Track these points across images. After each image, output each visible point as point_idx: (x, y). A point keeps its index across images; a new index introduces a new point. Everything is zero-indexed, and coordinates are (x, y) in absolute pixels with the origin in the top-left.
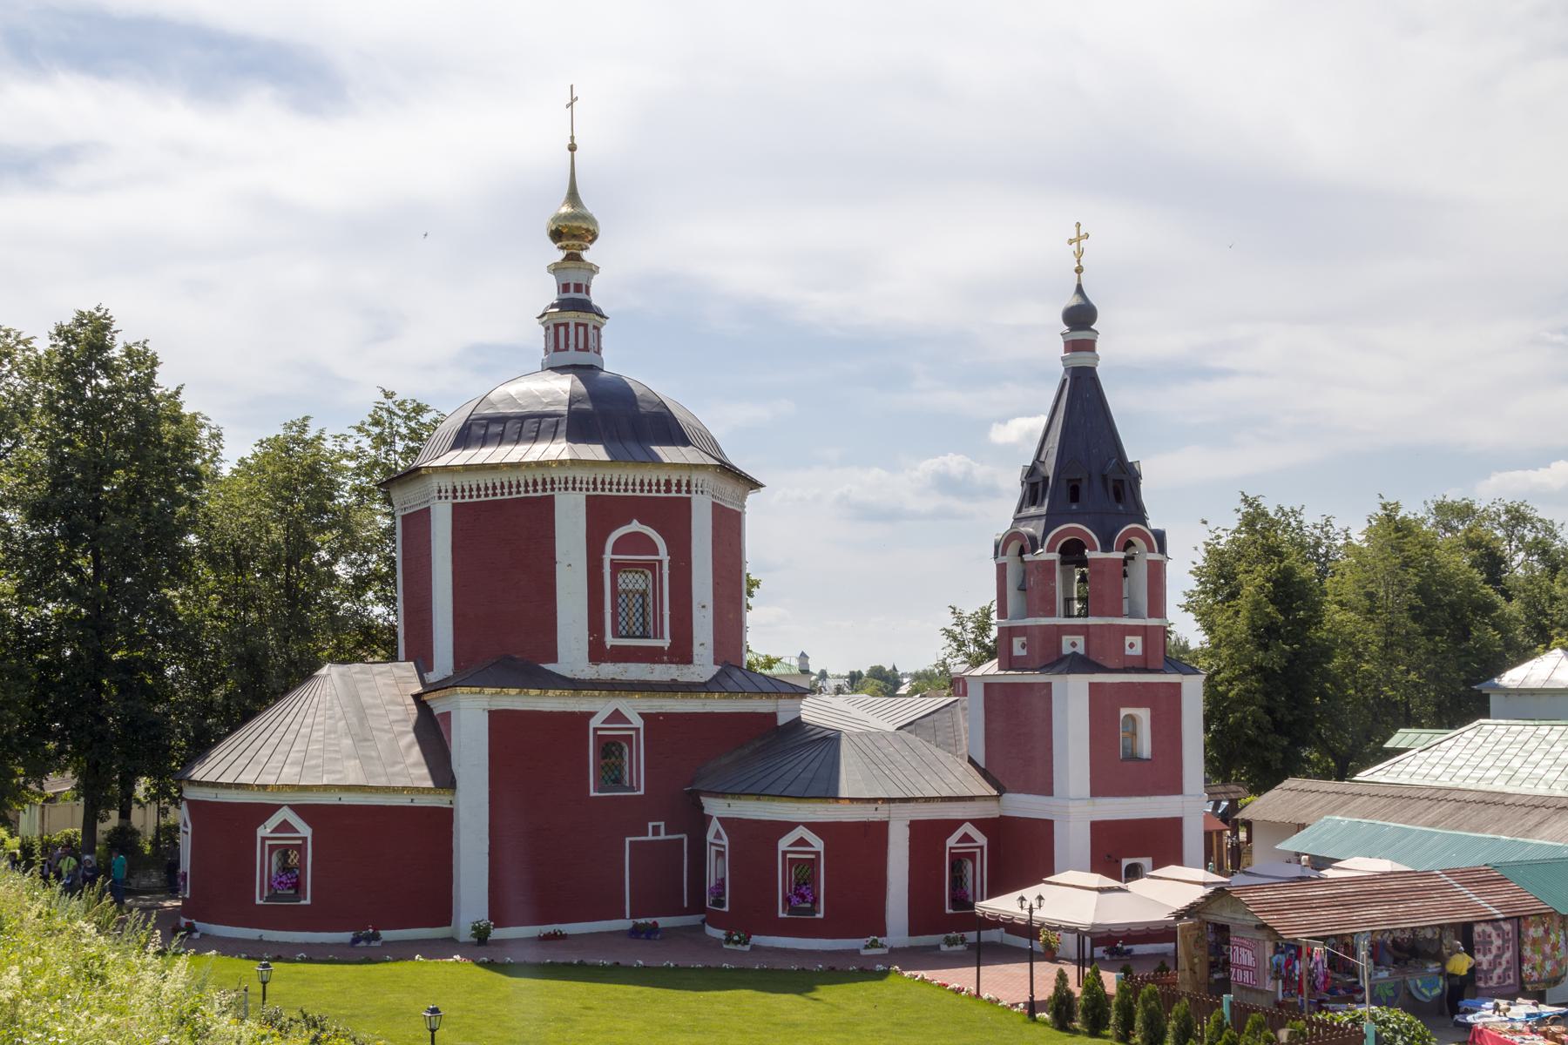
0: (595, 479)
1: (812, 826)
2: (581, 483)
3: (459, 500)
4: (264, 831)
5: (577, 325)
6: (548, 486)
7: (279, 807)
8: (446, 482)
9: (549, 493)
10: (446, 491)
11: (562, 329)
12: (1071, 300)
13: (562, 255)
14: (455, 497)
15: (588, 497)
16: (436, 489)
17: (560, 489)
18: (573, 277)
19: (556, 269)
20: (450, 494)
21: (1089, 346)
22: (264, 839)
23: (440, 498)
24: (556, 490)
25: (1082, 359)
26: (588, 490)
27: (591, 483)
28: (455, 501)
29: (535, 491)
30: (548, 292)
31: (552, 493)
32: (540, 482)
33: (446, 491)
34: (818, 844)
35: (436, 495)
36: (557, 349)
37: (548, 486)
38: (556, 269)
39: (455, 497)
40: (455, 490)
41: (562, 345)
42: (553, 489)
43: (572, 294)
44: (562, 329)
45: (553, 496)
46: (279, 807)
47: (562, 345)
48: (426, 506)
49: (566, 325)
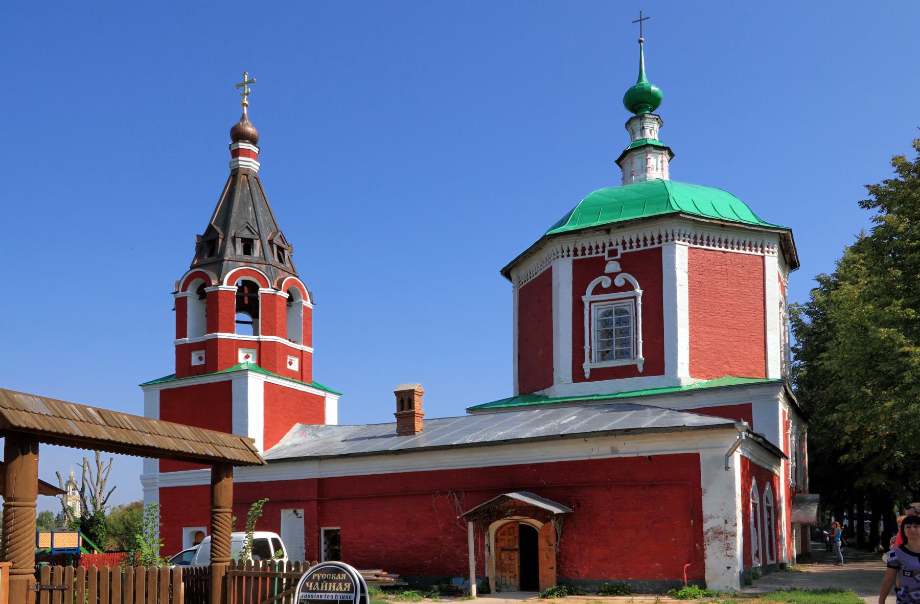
0: (695, 236)
2: (684, 236)
3: (580, 257)
6: (656, 241)
8: (569, 243)
9: (656, 245)
10: (569, 251)
14: (576, 254)
15: (690, 248)
16: (559, 250)
17: (667, 241)
20: (571, 253)
23: (563, 256)
24: (664, 242)
26: (689, 242)
27: (692, 238)
28: (576, 258)
29: (646, 245)
31: (659, 246)
32: (649, 238)
33: (569, 251)
35: (560, 254)
37: (656, 241)
39: (576, 254)
40: (576, 250)
42: (660, 242)
45: (660, 249)
48: (549, 266)
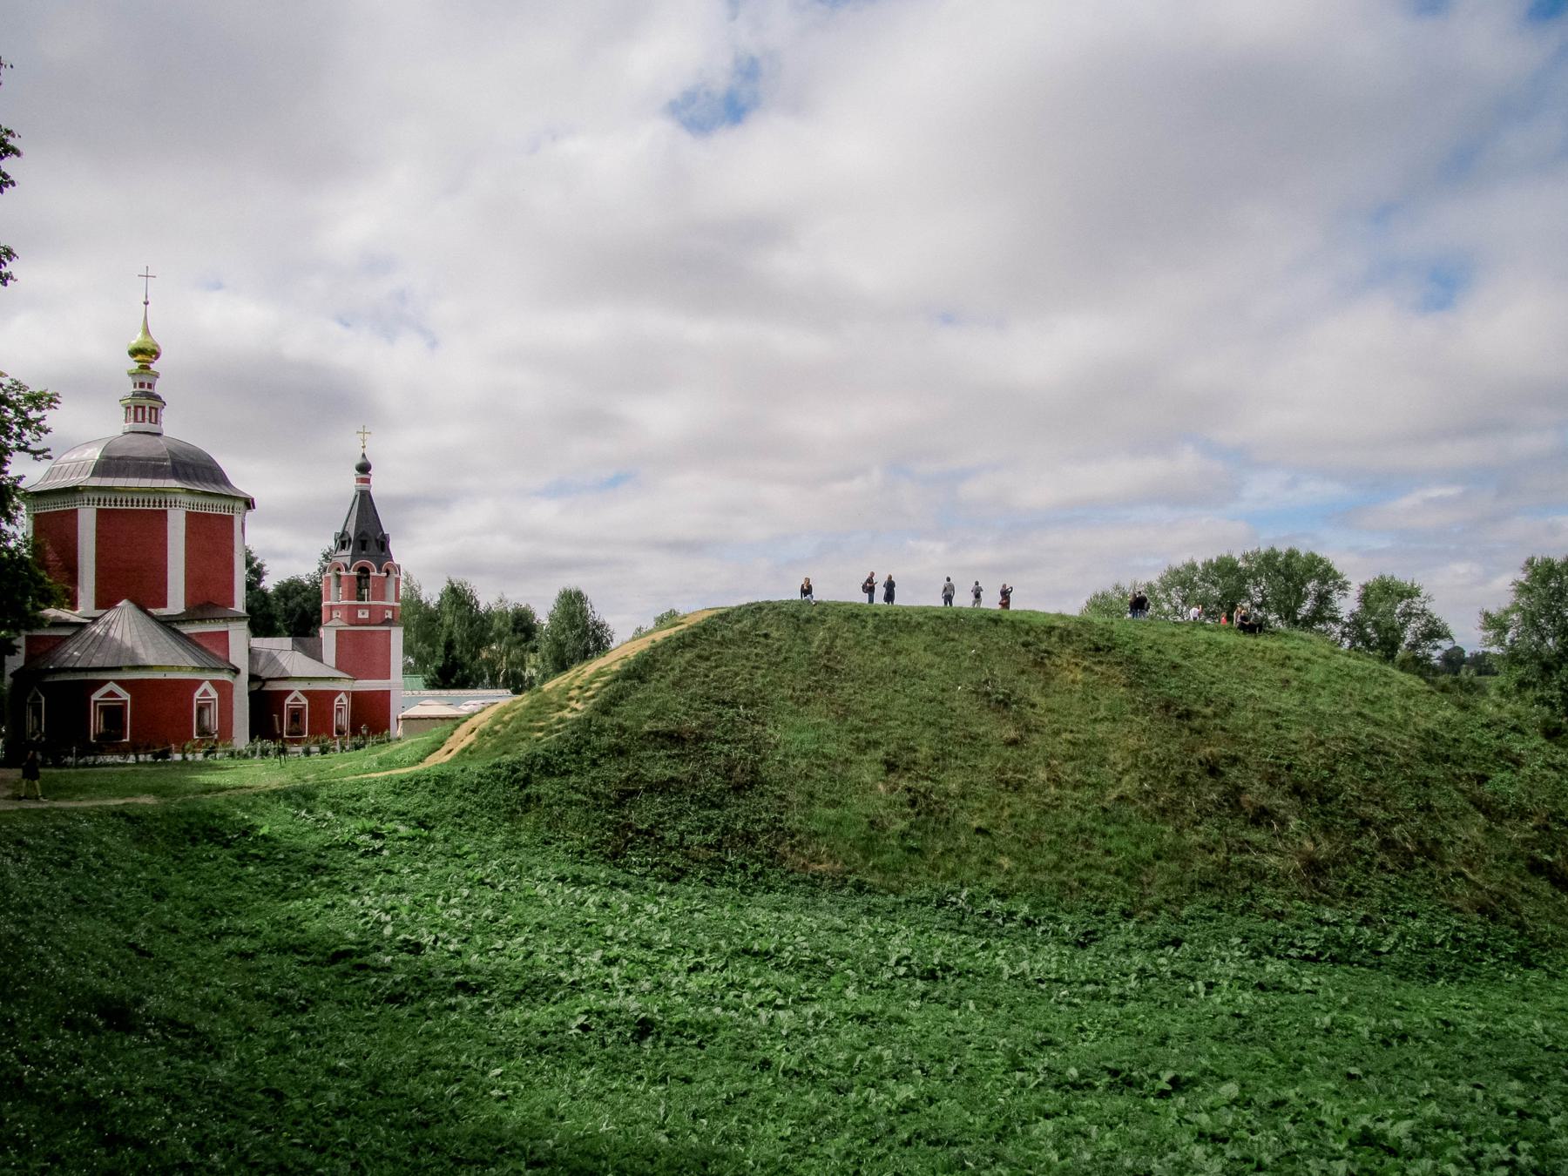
1: (305, 693)
4: (95, 697)
5: (151, 408)
7: (107, 681)
11: (140, 410)
12: (359, 460)
13: (138, 365)
18: (146, 381)
19: (132, 374)
21: (368, 481)
22: (96, 702)
25: (364, 486)
30: (129, 388)
34: (305, 701)
36: (136, 420)
38: (132, 374)
41: (140, 418)
43: (146, 389)
44: (140, 410)
46: (106, 682)
47: (140, 418)
49: (144, 408)
